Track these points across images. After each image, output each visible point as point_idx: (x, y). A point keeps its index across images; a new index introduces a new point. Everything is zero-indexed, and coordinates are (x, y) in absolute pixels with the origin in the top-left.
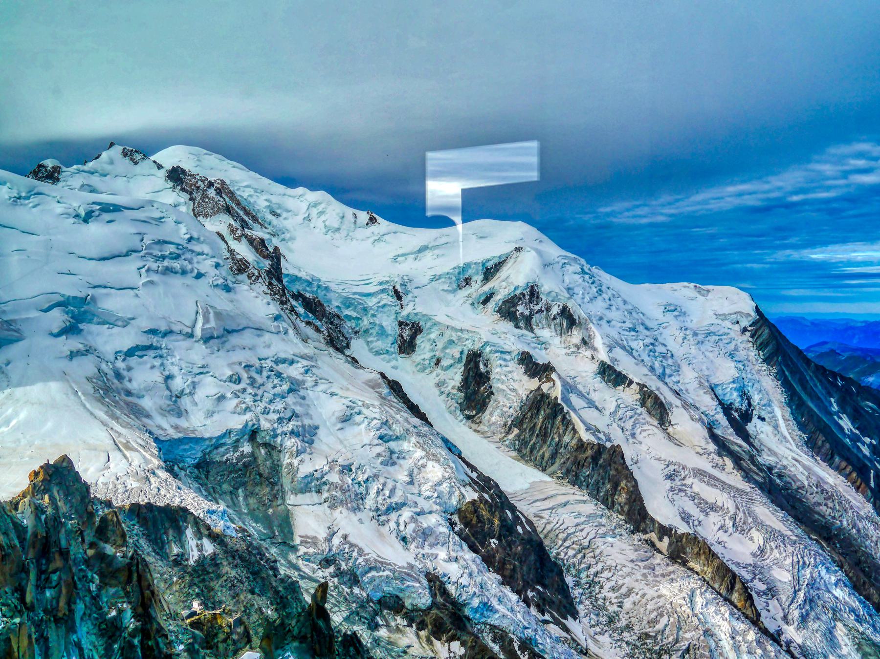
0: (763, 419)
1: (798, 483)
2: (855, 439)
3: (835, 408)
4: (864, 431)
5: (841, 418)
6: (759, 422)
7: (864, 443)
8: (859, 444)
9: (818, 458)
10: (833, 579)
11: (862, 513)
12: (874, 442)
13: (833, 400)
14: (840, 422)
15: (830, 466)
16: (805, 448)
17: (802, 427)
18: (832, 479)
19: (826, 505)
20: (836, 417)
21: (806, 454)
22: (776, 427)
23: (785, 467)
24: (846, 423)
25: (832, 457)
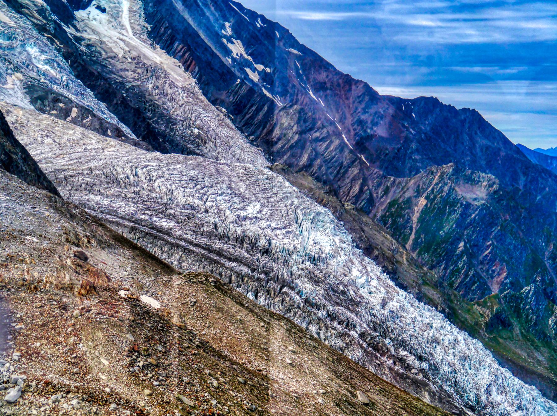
0: (103, 11)
1: (112, 54)
2: (242, 64)
3: (229, 31)
4: (258, 57)
5: (232, 43)
6: (98, 12)
7: (254, 70)
8: (248, 70)
9: (158, 46)
10: (43, 57)
11: (180, 84)
12: (268, 70)
13: (227, 24)
14: (230, 46)
15: (168, 53)
16: (145, 37)
17: (149, 17)
18: (157, 56)
19: (134, 71)
20: (225, 41)
21: (142, 40)
22: (116, 16)
23: (101, 42)
24: (237, 49)
25: (172, 43)
